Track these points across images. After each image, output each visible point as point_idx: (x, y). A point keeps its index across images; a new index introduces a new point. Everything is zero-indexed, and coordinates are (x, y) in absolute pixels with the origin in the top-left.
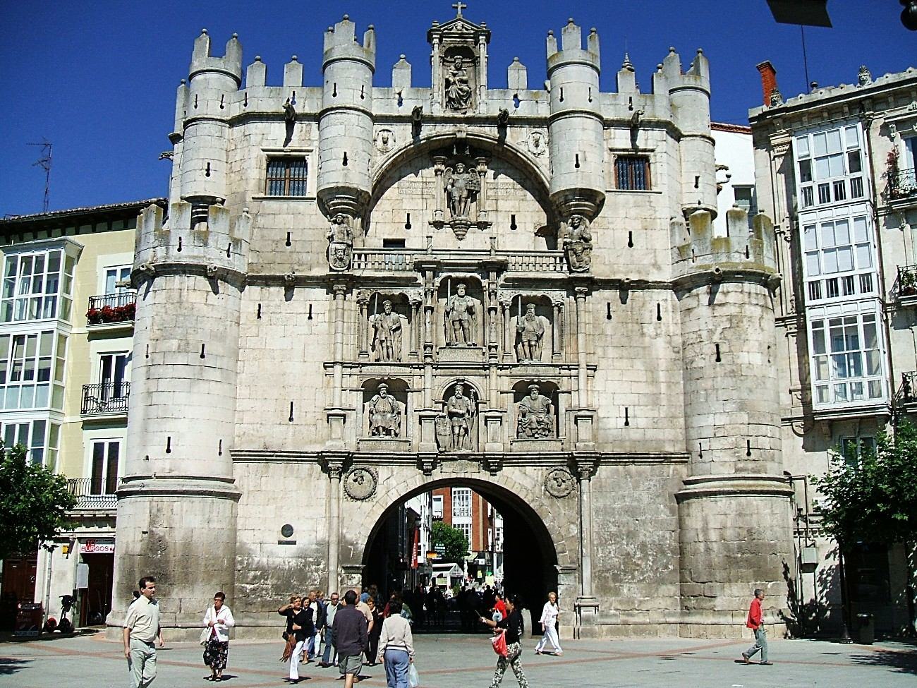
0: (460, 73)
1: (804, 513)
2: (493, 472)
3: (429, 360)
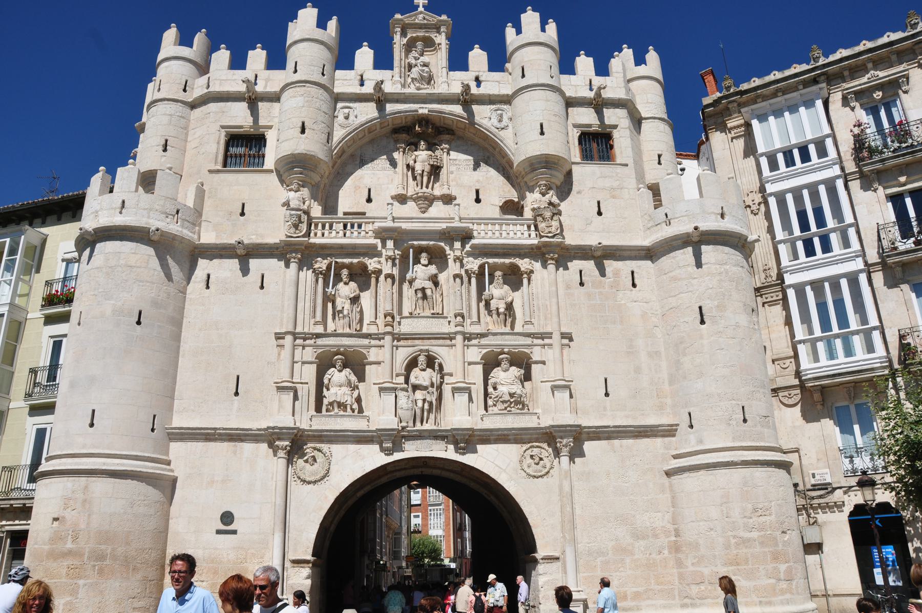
0: (422, 58)
1: (801, 488)
3: (389, 329)
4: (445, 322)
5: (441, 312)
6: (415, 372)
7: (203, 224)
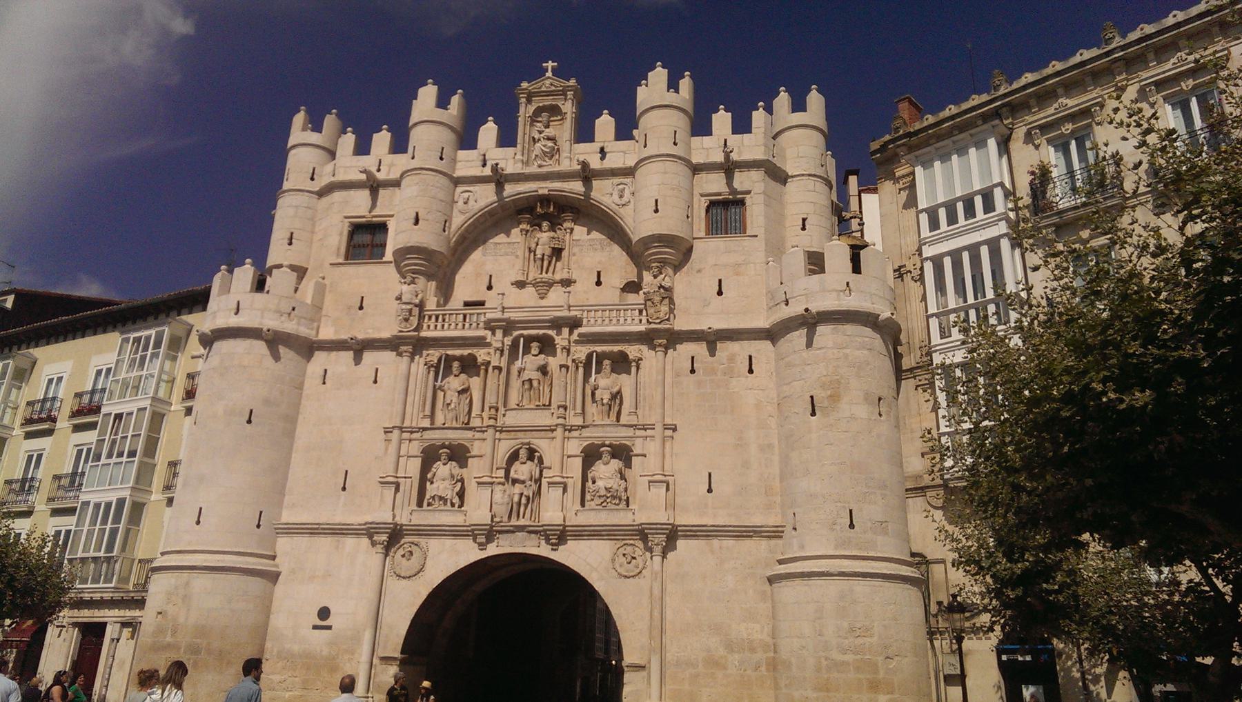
0: (547, 130)
2: (555, 547)
3: (492, 422)
4: (547, 413)
5: (547, 404)
6: (516, 466)
7: (323, 319)
